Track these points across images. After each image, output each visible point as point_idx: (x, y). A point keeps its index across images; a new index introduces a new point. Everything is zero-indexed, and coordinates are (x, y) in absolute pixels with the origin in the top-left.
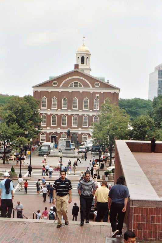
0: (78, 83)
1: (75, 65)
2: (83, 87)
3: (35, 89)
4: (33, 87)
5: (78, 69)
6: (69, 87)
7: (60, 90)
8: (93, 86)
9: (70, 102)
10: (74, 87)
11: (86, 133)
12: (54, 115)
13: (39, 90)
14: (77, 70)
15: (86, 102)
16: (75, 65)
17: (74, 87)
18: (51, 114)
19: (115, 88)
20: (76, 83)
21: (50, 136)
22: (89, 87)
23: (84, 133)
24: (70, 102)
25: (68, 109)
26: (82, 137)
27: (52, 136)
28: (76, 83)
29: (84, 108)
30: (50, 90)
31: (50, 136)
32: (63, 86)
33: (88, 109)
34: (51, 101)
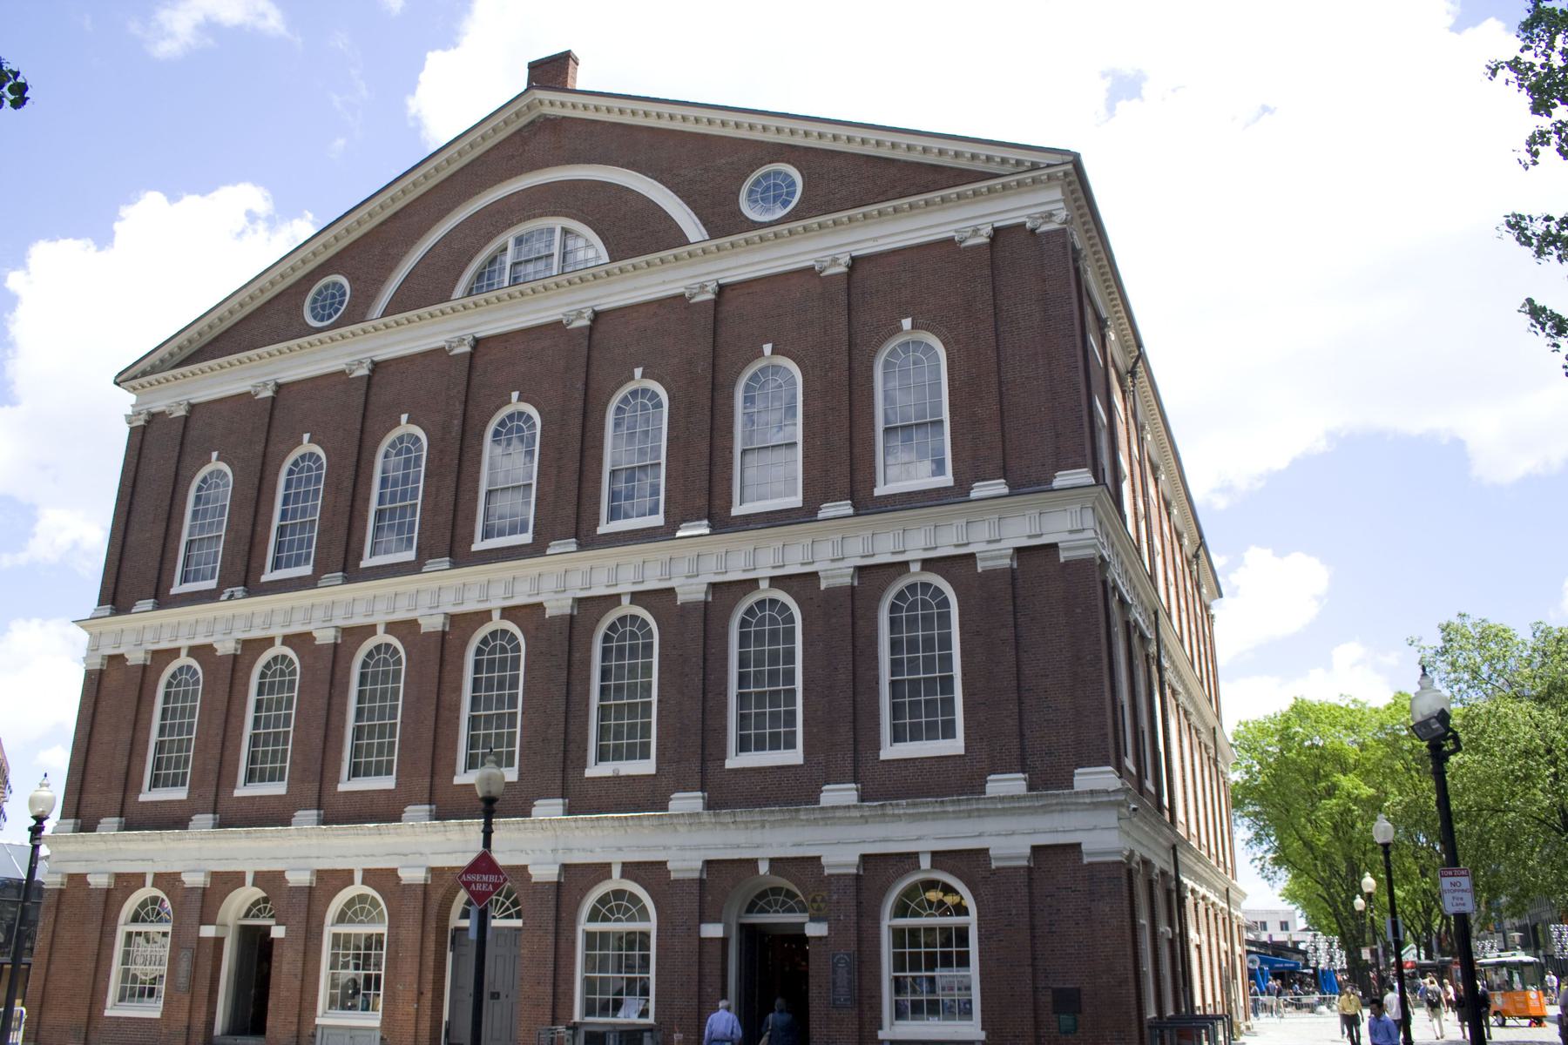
11: (632, 870)
13: (173, 397)
22: (676, 237)
33: (658, 520)
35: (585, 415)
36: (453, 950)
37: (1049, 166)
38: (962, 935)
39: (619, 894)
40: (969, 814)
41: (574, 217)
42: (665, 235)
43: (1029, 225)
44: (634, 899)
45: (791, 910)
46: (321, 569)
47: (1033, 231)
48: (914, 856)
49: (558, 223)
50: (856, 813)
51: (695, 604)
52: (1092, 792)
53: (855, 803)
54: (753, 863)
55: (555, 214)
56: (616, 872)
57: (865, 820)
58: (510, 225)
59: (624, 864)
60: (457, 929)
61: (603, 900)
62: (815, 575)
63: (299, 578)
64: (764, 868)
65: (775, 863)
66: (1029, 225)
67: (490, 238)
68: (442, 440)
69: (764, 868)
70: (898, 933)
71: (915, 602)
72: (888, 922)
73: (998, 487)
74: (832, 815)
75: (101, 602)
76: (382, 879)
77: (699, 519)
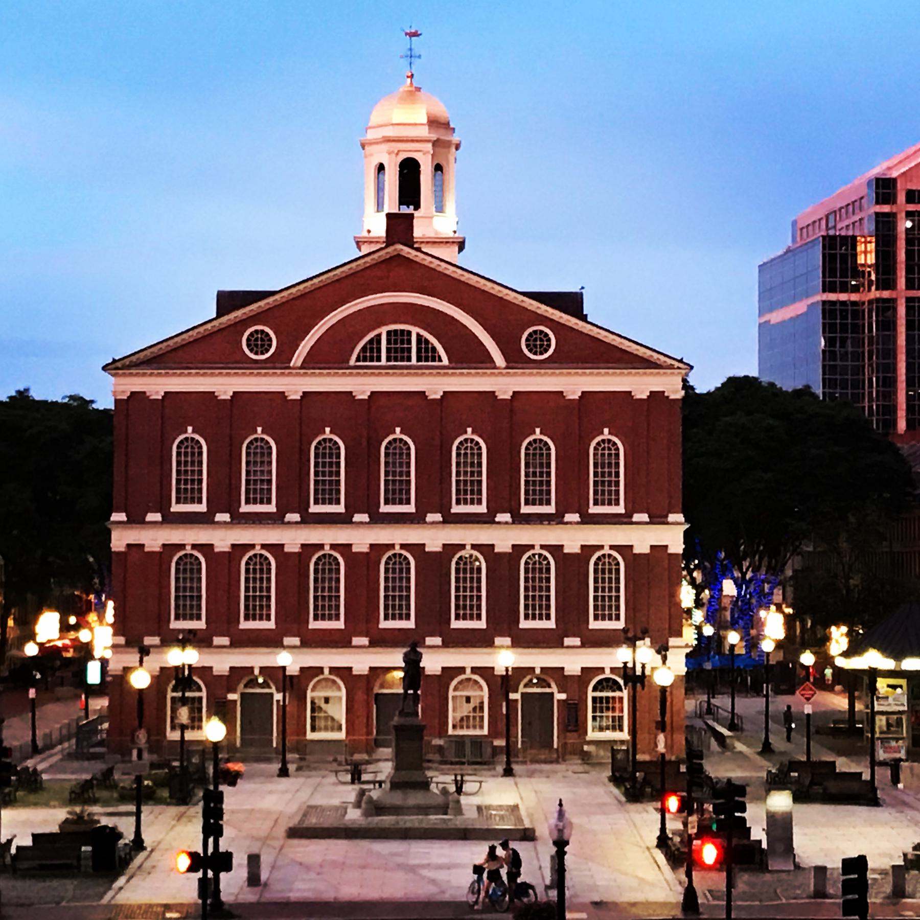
2: (445, 362)
3: (122, 380)
6: (352, 362)
10: (384, 362)
11: (475, 670)
14: (406, 251)
15: (470, 453)
17: (384, 362)
19: (656, 366)
20: (399, 340)
21: (232, 696)
23: (462, 670)
26: (451, 693)
27: (243, 695)
28: (399, 340)
29: (458, 502)
31: (232, 696)
33: (482, 509)
36: (376, 704)
37: (679, 368)
39: (469, 680)
41: (425, 329)
42: (484, 360)
43: (666, 394)
44: (476, 682)
46: (283, 510)
47: (668, 397)
60: (377, 695)
61: (460, 683)
65: (542, 669)
66: (666, 394)
70: (594, 699)
71: (605, 562)
72: (590, 694)
73: (645, 517)
76: (344, 673)
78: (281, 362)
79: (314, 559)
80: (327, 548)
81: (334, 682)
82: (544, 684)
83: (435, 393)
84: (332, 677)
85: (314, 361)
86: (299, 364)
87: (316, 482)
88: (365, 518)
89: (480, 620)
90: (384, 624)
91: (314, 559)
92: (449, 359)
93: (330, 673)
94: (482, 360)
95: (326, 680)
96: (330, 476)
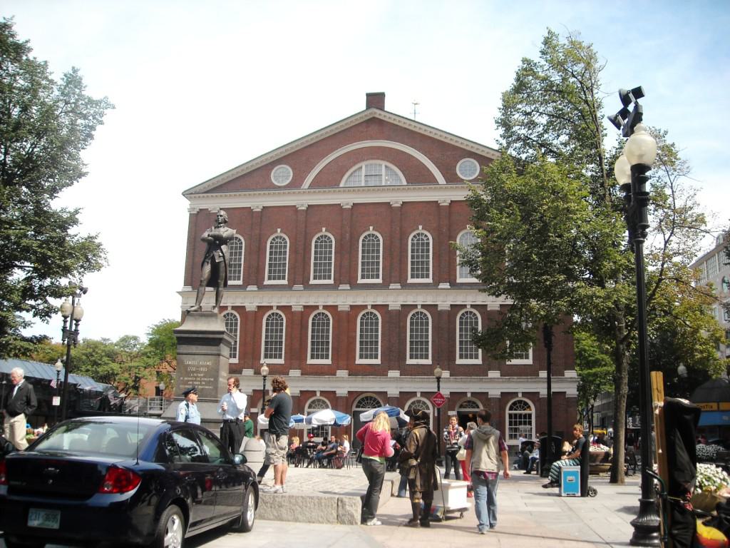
0: (383, 167)
1: (368, 95)
2: (404, 182)
4: (188, 194)
5: (382, 108)
7: (302, 200)
8: (452, 178)
9: (346, 249)
12: (275, 310)
13: (216, 204)
15: (421, 246)
16: (368, 95)
18: (259, 307)
22: (434, 181)
24: (346, 249)
25: (338, 282)
30: (257, 202)
32: (314, 185)
34: (261, 250)
35: (401, 239)
38: (530, 416)
40: (535, 382)
41: (391, 162)
42: (431, 180)
45: (474, 407)
48: (517, 393)
49: (384, 163)
50: (501, 380)
51: (445, 311)
52: (571, 378)
53: (500, 377)
54: (465, 394)
55: (382, 159)
56: (419, 395)
57: (503, 382)
58: (364, 160)
59: (421, 392)
62: (486, 305)
63: (281, 285)
64: (469, 395)
67: (355, 164)
68: (341, 240)
69: (469, 395)
72: (507, 412)
74: (492, 380)
75: (186, 284)
77: (446, 282)
78: (295, 184)
79: (312, 316)
80: (321, 308)
81: (324, 402)
82: (474, 405)
83: (397, 203)
84: (322, 398)
85: (317, 184)
86: (307, 186)
87: (315, 264)
88: (347, 287)
89: (428, 358)
90: (359, 361)
91: (312, 316)
92: (407, 181)
93: (321, 395)
94: (428, 179)
95: (319, 400)
96: (325, 260)
